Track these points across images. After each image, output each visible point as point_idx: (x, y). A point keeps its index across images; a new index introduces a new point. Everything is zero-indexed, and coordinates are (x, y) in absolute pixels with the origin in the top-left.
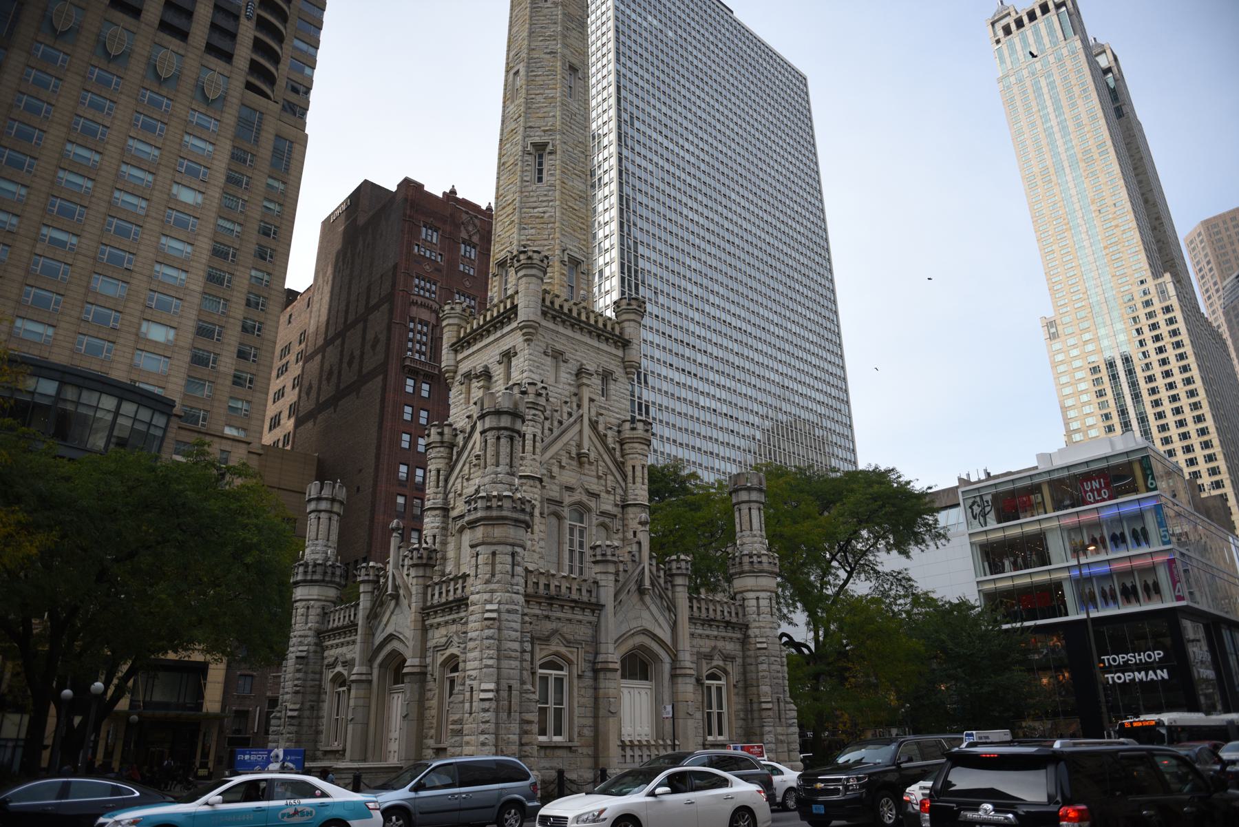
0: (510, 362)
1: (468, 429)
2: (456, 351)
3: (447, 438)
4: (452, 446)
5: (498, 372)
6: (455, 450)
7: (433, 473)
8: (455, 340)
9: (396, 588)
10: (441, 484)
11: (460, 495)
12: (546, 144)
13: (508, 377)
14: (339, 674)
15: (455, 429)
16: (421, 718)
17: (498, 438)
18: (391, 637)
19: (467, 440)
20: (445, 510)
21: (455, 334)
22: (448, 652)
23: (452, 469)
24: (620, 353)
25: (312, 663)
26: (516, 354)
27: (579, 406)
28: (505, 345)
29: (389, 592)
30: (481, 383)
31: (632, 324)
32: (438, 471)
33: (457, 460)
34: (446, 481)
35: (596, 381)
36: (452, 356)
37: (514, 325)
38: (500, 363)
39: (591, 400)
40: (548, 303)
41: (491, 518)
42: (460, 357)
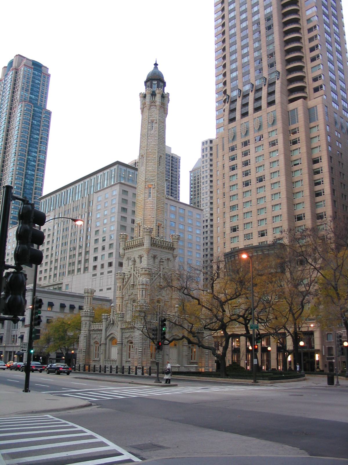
0: (141, 258)
2: (124, 249)
3: (122, 277)
5: (138, 260)
7: (119, 287)
9: (113, 321)
13: (141, 262)
14: (96, 341)
16: (122, 354)
18: (112, 334)
19: (129, 278)
21: (124, 244)
22: (129, 339)
23: (124, 286)
24: (172, 252)
25: (89, 338)
27: (160, 271)
28: (140, 253)
29: (111, 322)
31: (176, 242)
35: (165, 262)
36: (123, 250)
37: (142, 248)
39: (163, 268)
40: (152, 242)
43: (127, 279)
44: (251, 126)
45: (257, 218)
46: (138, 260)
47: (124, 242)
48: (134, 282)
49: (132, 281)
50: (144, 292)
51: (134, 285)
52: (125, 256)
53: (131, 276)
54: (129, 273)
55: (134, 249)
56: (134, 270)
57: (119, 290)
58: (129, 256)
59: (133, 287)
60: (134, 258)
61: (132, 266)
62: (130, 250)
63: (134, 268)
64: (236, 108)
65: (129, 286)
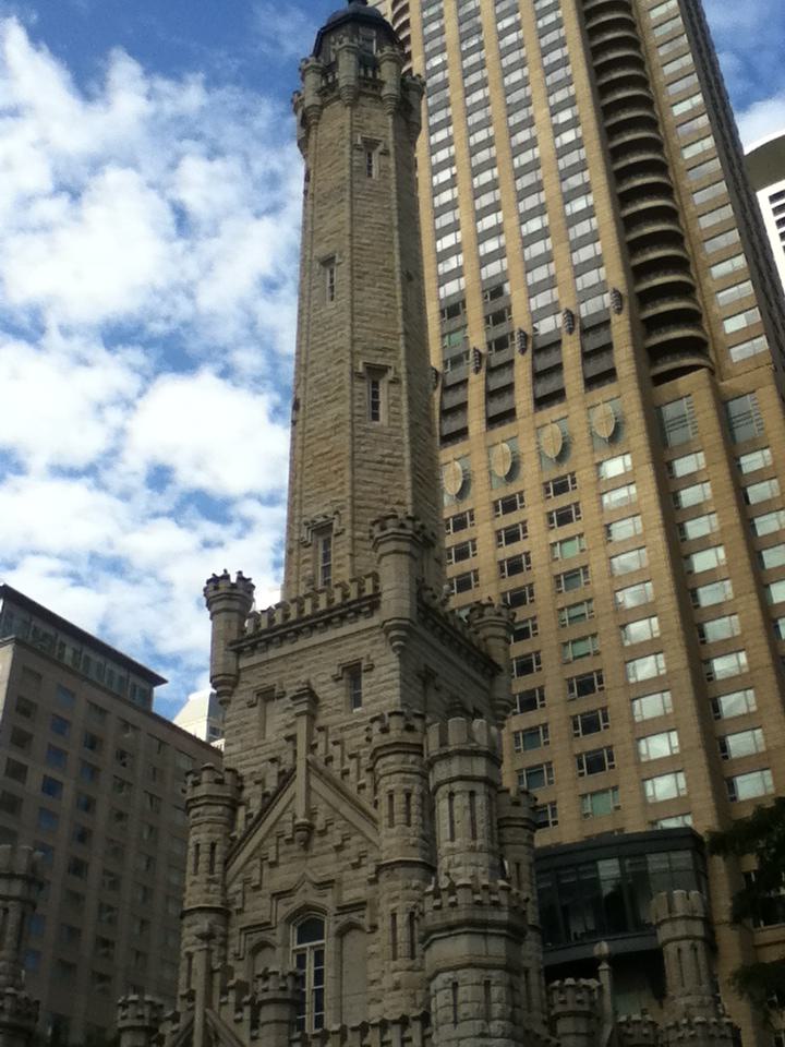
1: (272, 784)
2: (239, 652)
4: (234, 805)
5: (332, 693)
6: (242, 812)
7: (205, 848)
8: (234, 636)
10: (218, 868)
11: (257, 888)
12: (383, 370)
13: (356, 701)
15: (240, 778)
17: (472, 794)
19: (269, 800)
20: (224, 913)
21: (235, 626)
23: (234, 847)
26: (371, 668)
30: (304, 707)
32: (213, 846)
33: (250, 831)
34: (226, 863)
36: (231, 657)
38: (337, 679)
41: (485, 924)
42: (244, 663)
43: (256, 805)
44: (527, 447)
45: (571, 747)
46: (332, 693)
47: (236, 615)
48: (311, 813)
49: (300, 809)
50: (480, 800)
51: (309, 828)
52: (242, 687)
53: (286, 778)
54: (274, 770)
55: (303, 643)
56: (312, 748)
57: (203, 866)
58: (269, 681)
59: (306, 845)
60: (308, 683)
61: (301, 729)
62: (272, 653)
63: (310, 736)
64: (466, 403)
65: (272, 841)
